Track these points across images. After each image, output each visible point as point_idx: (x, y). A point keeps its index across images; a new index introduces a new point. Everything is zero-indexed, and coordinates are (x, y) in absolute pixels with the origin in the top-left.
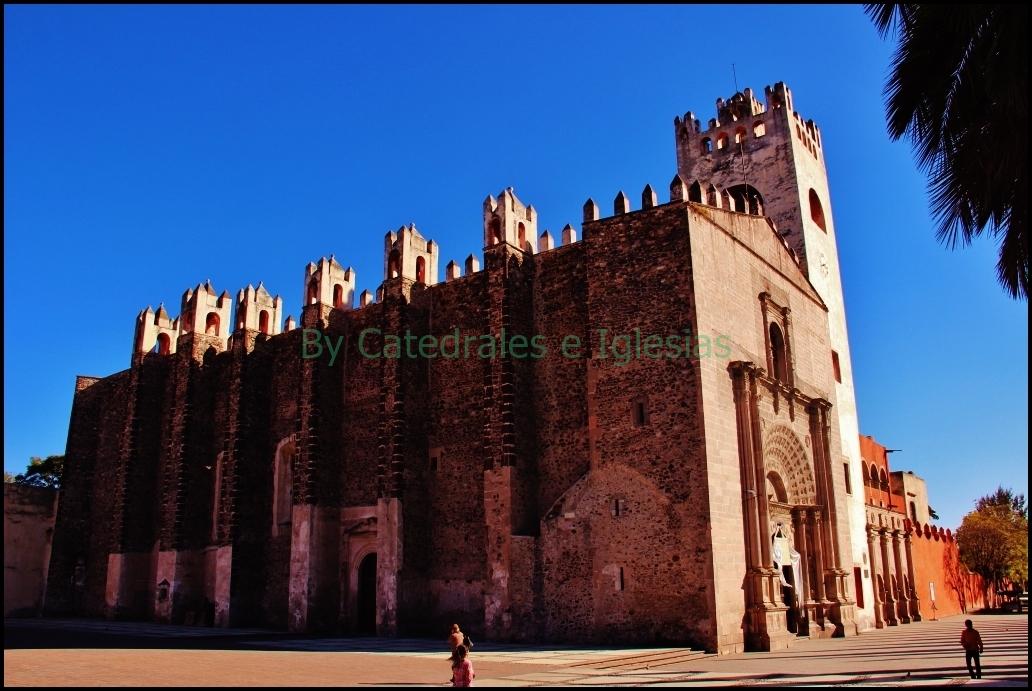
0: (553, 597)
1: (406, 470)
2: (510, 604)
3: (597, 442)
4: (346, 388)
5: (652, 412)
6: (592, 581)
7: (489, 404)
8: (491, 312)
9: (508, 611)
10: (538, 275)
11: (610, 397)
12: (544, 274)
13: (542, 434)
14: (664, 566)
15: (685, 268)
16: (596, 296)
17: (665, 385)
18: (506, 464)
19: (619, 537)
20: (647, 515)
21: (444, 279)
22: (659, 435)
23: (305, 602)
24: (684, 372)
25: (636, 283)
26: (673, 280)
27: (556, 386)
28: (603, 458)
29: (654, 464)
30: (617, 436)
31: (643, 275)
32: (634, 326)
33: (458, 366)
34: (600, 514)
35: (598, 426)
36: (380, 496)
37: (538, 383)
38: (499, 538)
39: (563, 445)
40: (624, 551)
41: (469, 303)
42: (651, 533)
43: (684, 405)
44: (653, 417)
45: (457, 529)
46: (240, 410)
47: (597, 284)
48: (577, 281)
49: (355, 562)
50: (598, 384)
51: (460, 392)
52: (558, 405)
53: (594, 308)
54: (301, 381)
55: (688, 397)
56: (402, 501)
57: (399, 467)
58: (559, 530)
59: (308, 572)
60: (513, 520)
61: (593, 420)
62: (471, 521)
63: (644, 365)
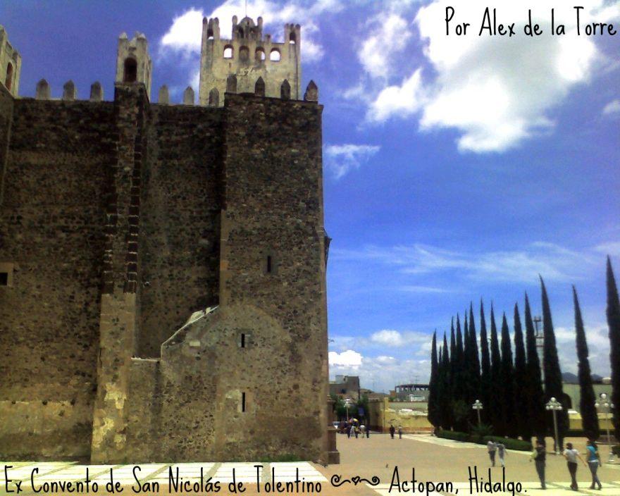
0: (172, 418)
7: (113, 231)
8: (119, 146)
9: (123, 432)
11: (242, 247)
14: (284, 393)
18: (130, 290)
19: (244, 365)
20: (271, 350)
21: (32, 93)
22: (285, 284)
24: (311, 238)
25: (273, 158)
26: (305, 163)
29: (280, 307)
30: (247, 280)
32: (268, 191)
33: (45, 186)
34: (227, 345)
35: (229, 269)
38: (117, 360)
40: (247, 377)
41: (64, 126)
43: (308, 264)
44: (281, 270)
48: (196, 139)
58: (183, 357)
61: (224, 265)
62: (52, 340)
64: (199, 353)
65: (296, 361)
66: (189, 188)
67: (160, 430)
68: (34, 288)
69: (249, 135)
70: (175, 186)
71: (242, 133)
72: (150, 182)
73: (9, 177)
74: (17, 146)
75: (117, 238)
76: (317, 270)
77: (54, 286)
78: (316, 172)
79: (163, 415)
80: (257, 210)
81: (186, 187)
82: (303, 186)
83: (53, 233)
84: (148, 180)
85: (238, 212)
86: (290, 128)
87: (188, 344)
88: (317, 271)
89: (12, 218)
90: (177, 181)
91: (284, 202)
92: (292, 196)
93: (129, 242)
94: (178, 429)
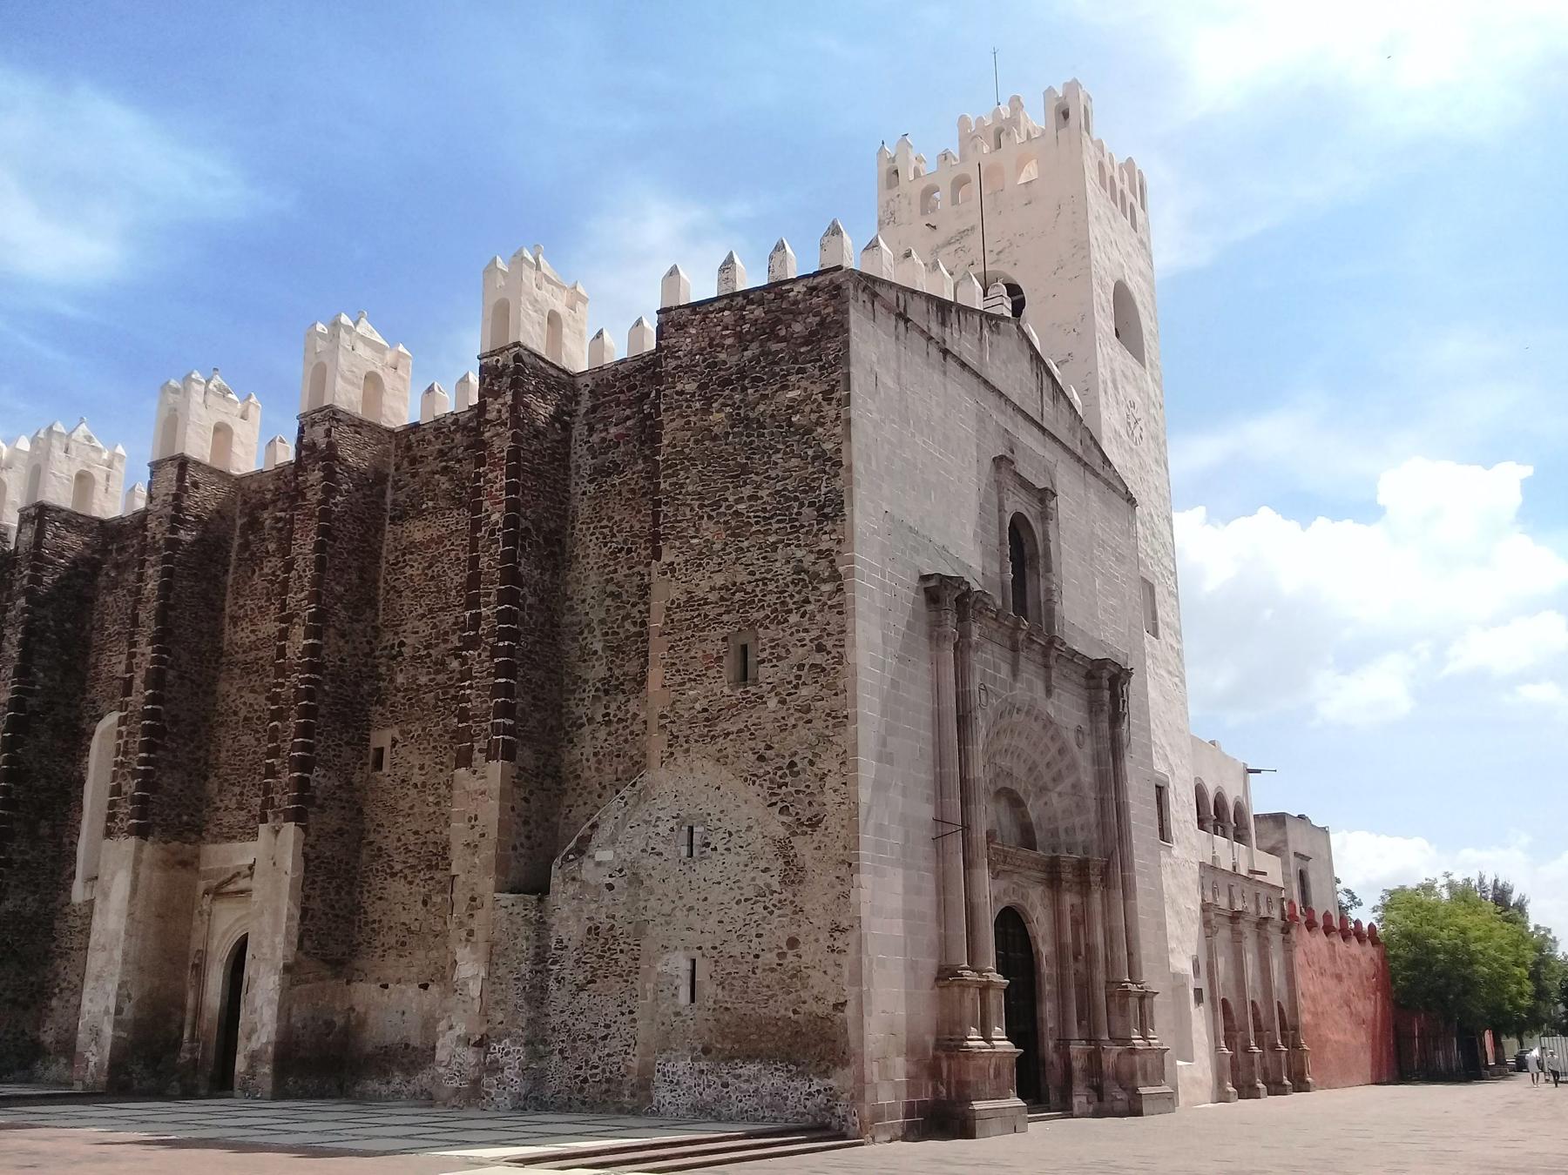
0: (565, 1016)
1: (318, 771)
2: (484, 1029)
3: (663, 717)
4: (232, 617)
5: (763, 661)
6: (638, 985)
7: (472, 643)
10: (584, 411)
12: (594, 409)
13: (572, 703)
14: (770, 958)
15: (836, 395)
16: (675, 446)
17: (790, 611)
18: (495, 758)
19: (690, 899)
20: (744, 858)
22: (772, 703)
23: (108, 1030)
24: (826, 588)
26: (814, 417)
27: (603, 615)
28: (670, 746)
29: (761, 758)
31: (761, 408)
32: (739, 501)
35: (664, 686)
36: (264, 820)
37: (571, 608)
38: (473, 899)
39: (608, 723)
40: (698, 927)
41: (459, 461)
42: (749, 892)
43: (820, 648)
44: (765, 671)
45: (411, 883)
46: (22, 657)
47: (680, 422)
49: (220, 952)
50: (668, 609)
51: (435, 626)
52: (605, 648)
53: (670, 467)
54: (139, 601)
55: (828, 635)
56: (305, 829)
57: (305, 765)
59: (118, 970)
60: (502, 866)
61: (656, 675)
63: (752, 573)
64: (611, 876)
65: (793, 882)
66: (637, 526)
67: (544, 1042)
68: (416, 770)
69: (702, 387)
70: (615, 529)
71: (691, 387)
72: (576, 531)
73: (389, 573)
74: (400, 517)
75: (479, 655)
76: (840, 660)
77: (442, 763)
78: (838, 430)
79: (550, 1010)
80: (717, 547)
81: (632, 527)
82: (811, 470)
83: (443, 663)
84: (573, 528)
85: (681, 559)
86: (784, 344)
87: (593, 857)
88: (840, 663)
89: (392, 647)
90: (617, 518)
91: (771, 518)
92: (788, 499)
93: (496, 660)
94: (574, 1041)
